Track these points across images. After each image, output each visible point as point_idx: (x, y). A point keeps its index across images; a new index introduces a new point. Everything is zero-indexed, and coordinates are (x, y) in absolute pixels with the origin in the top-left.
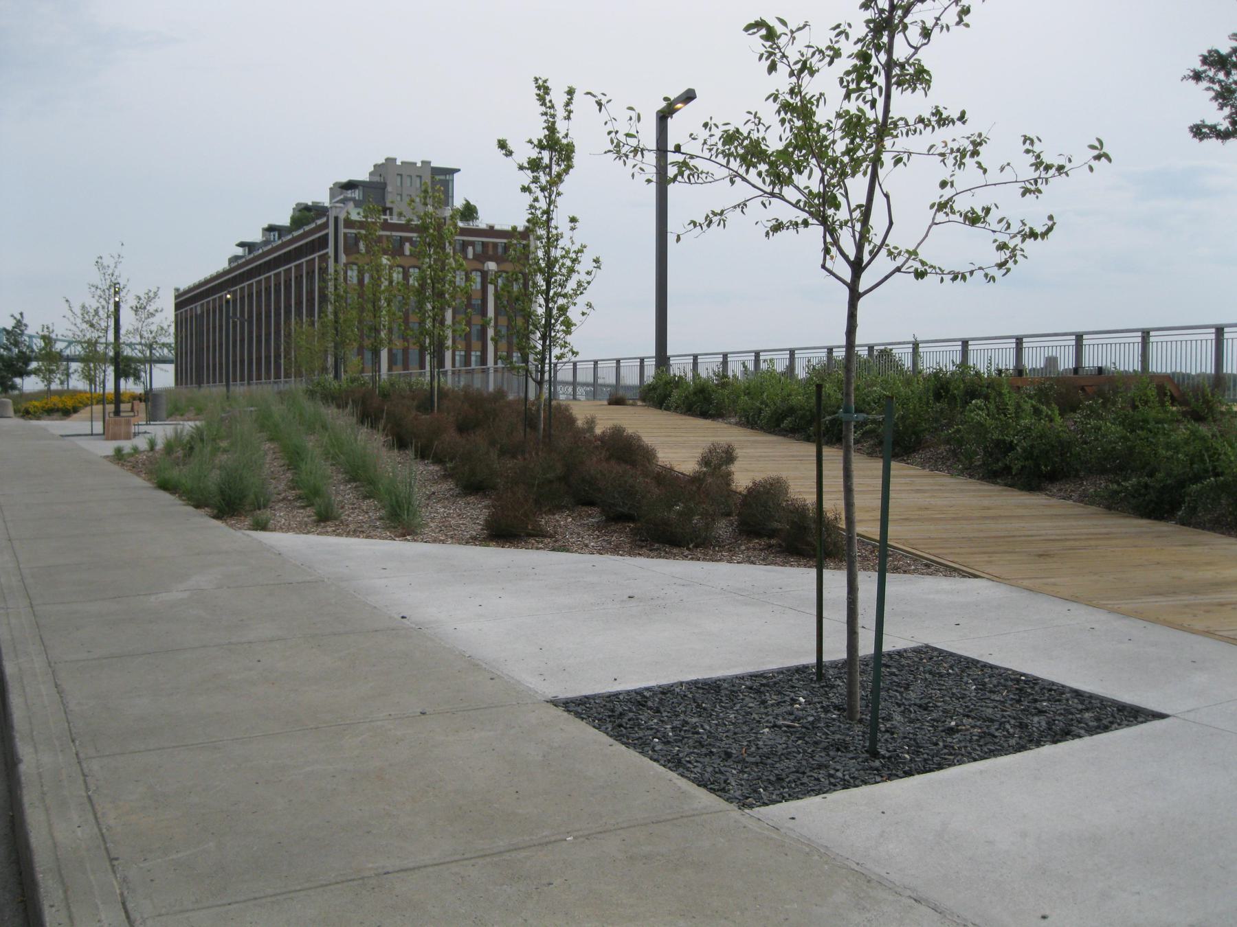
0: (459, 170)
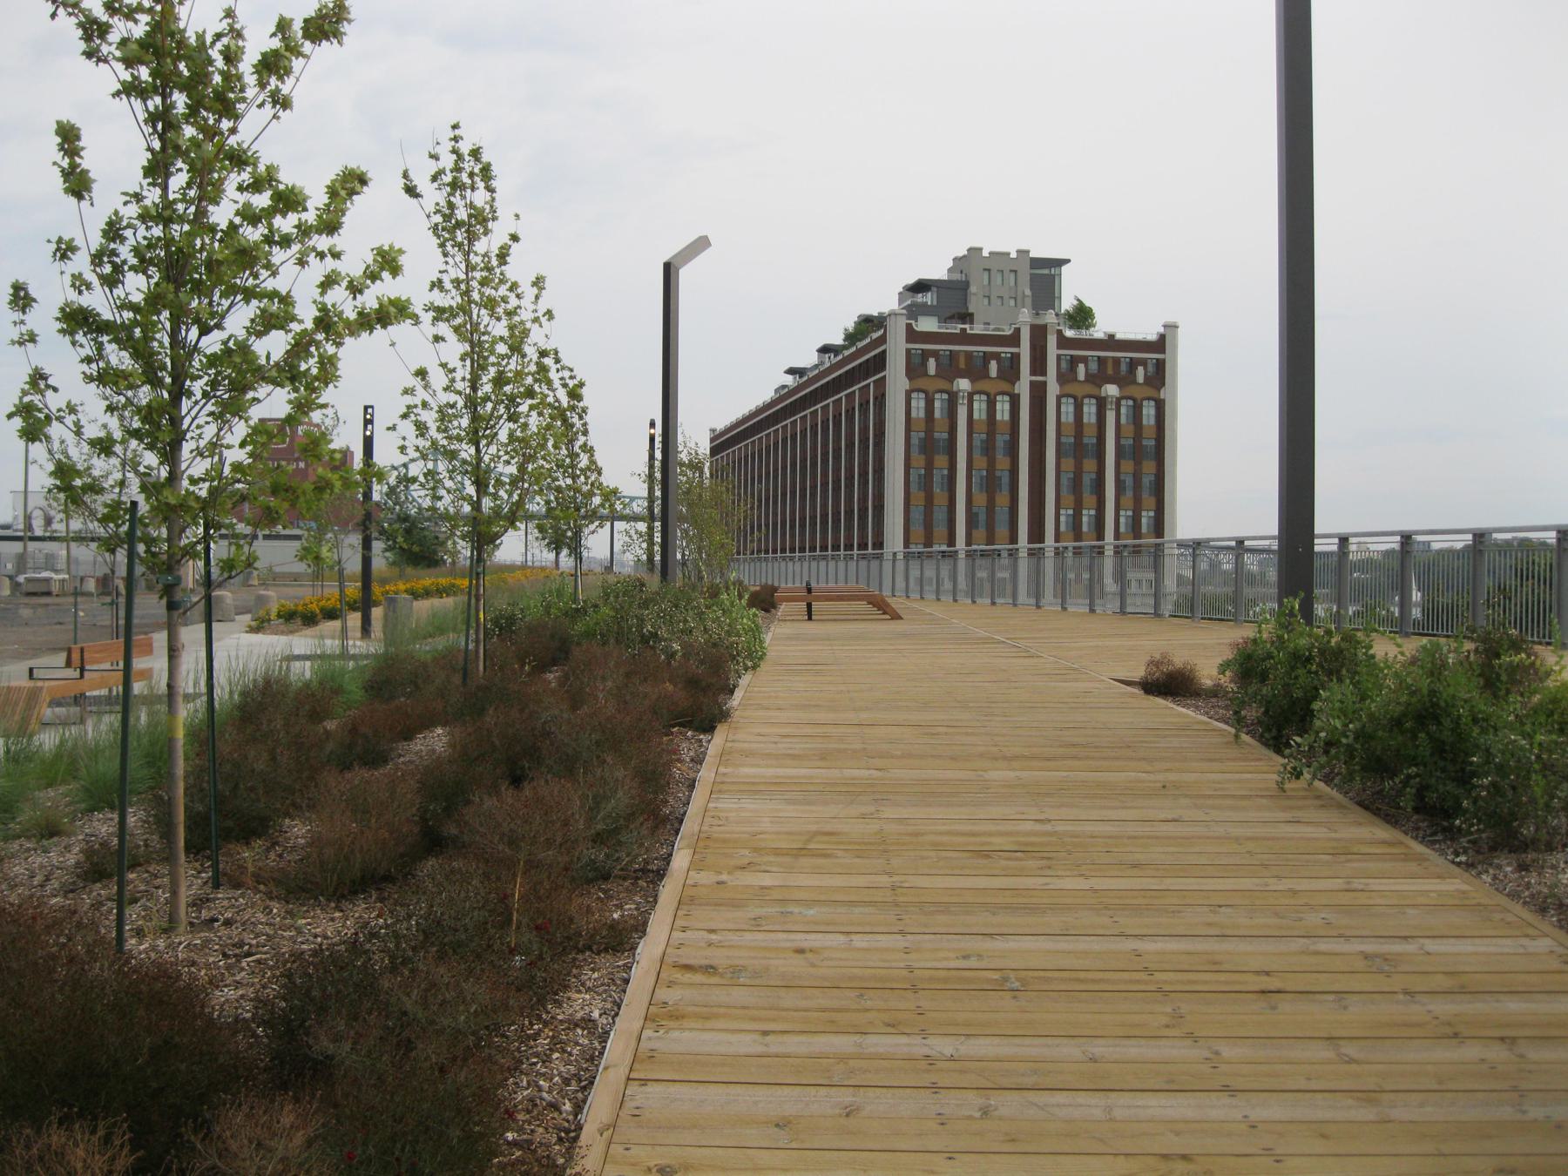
0: (1068, 261)
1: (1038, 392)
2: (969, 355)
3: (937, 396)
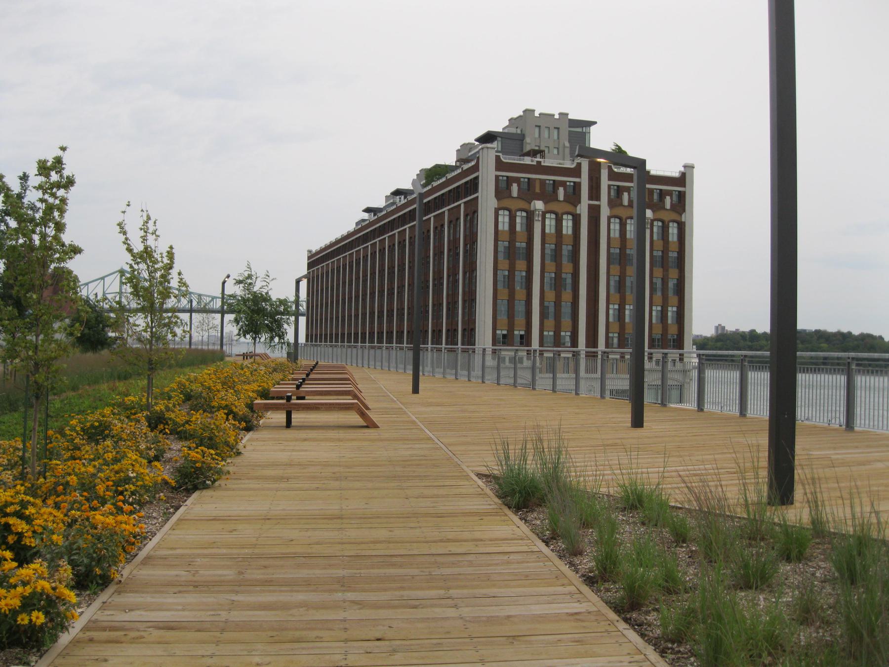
0: (595, 123)
1: (594, 213)
2: (543, 182)
3: (519, 213)
